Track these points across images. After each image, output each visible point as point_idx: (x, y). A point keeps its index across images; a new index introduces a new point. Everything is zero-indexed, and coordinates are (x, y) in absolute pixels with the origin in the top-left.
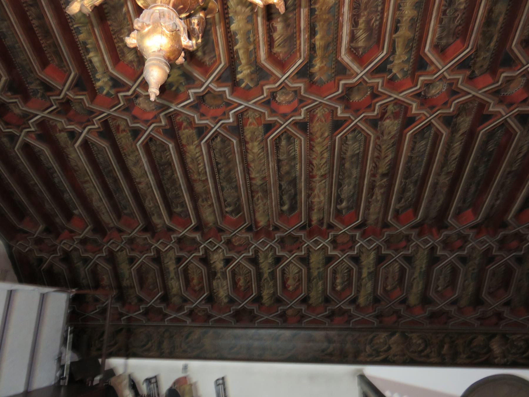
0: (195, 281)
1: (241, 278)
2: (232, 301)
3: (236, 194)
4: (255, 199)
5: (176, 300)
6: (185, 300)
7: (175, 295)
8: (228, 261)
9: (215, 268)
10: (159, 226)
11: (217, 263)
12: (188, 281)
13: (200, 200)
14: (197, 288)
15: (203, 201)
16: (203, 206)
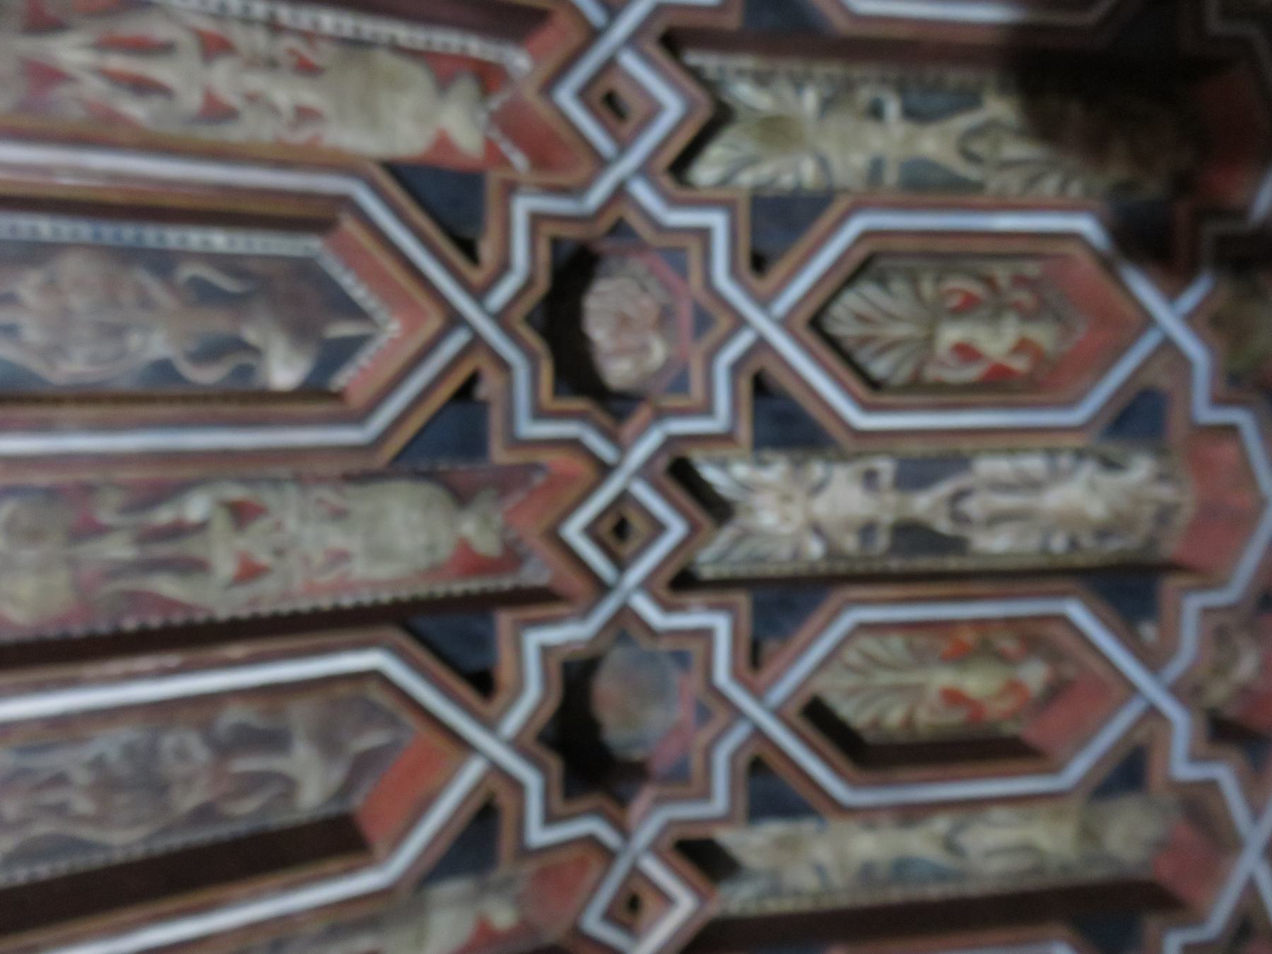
0: (978, 683)
1: (951, 334)
2: (1139, 419)
3: (72, 266)
4: (136, 110)
5: (1130, 837)
6: (1129, 772)
7: (1088, 834)
8: (783, 423)
9: (867, 530)
10: (503, 916)
11: (821, 507)
12: (975, 746)
13: (168, 586)
14: (1034, 675)
15: (193, 567)
16: (250, 572)
